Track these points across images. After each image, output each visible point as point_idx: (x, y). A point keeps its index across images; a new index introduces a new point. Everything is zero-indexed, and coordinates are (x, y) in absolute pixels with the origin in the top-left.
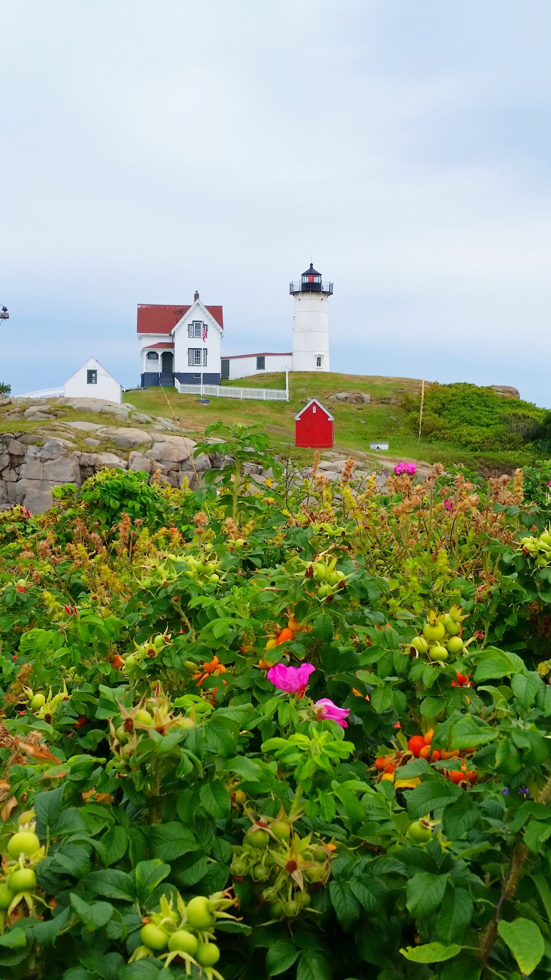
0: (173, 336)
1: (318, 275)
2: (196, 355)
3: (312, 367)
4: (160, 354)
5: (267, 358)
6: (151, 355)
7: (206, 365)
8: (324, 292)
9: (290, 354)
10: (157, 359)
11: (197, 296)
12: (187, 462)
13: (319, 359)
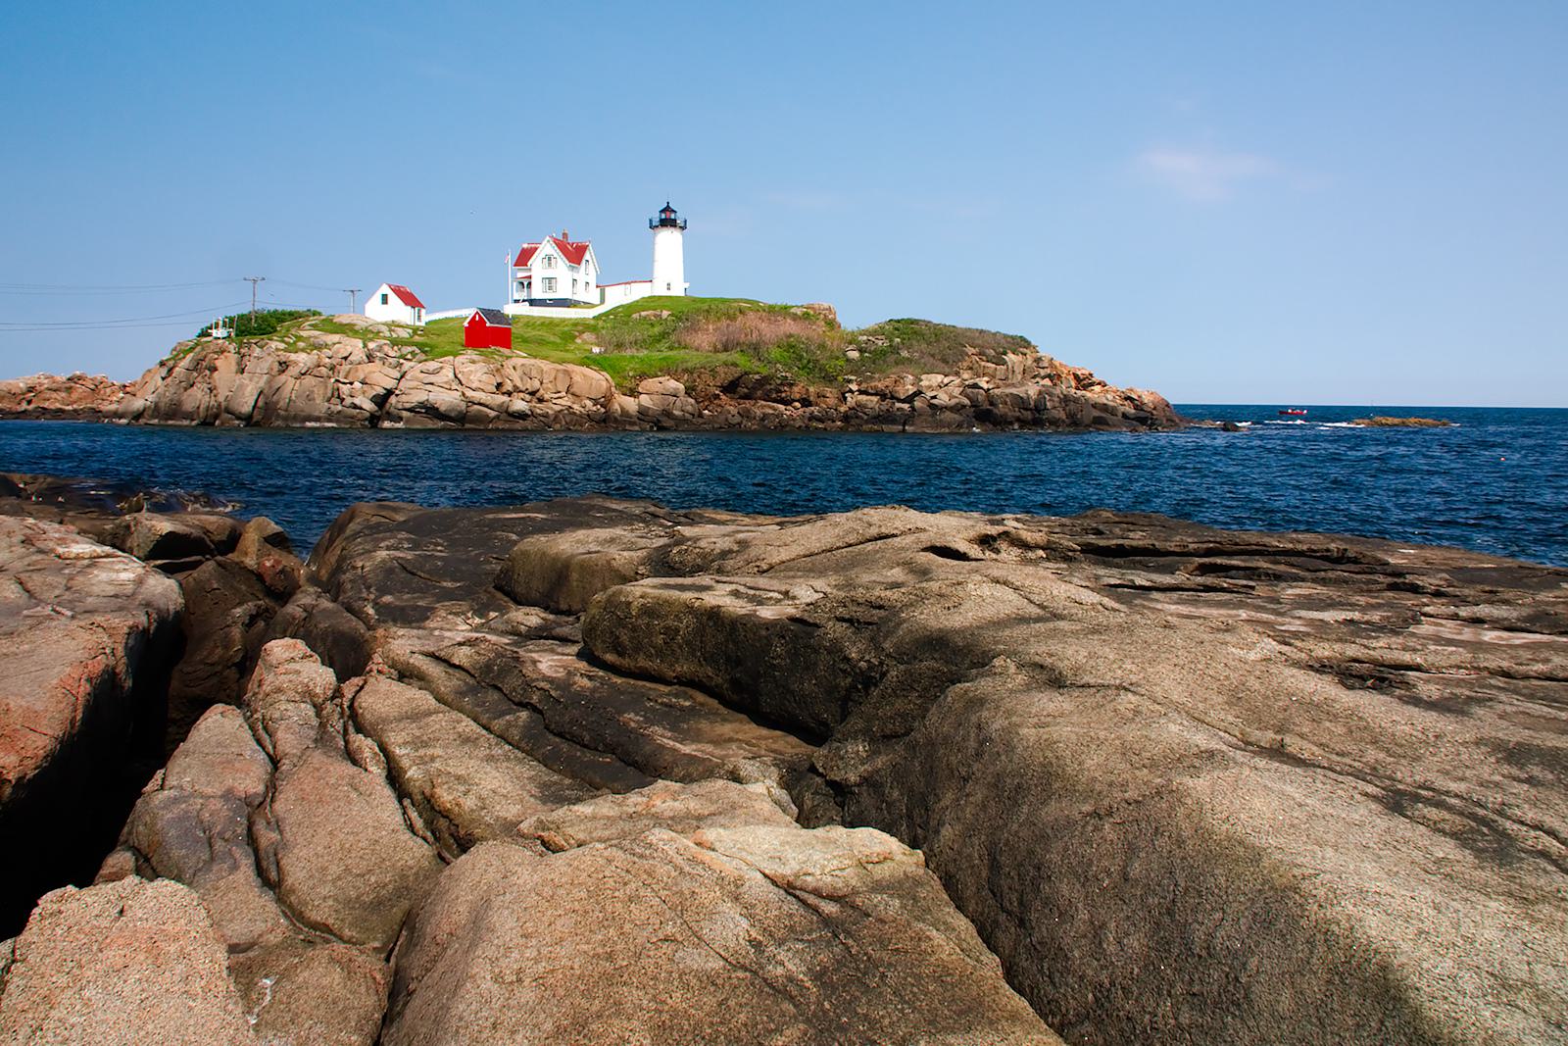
2: (550, 281)
3: (665, 293)
4: (526, 284)
11: (565, 235)
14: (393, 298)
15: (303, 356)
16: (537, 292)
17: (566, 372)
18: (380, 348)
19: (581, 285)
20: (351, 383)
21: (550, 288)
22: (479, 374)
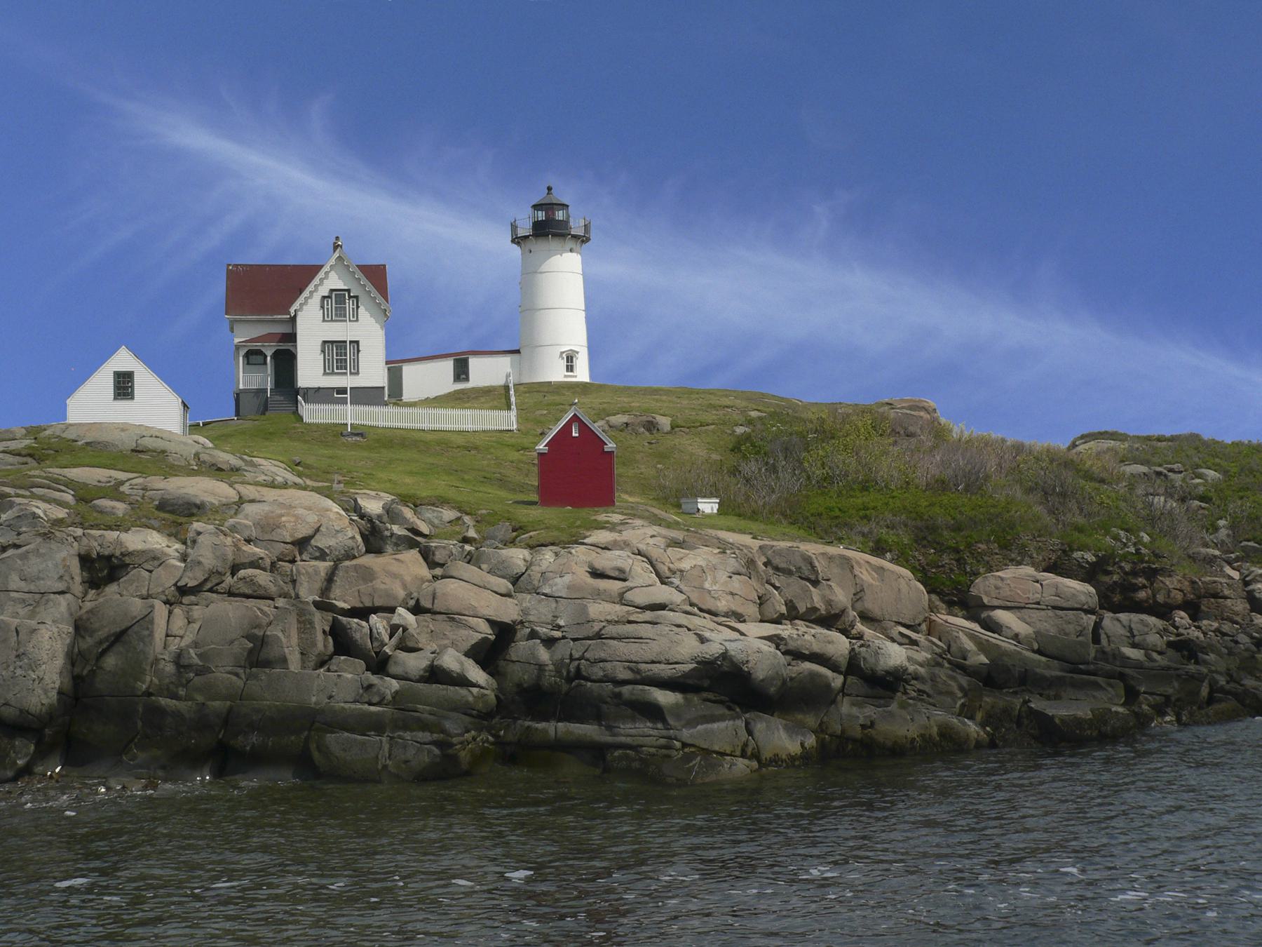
0: (293, 320)
1: (564, 206)
4: (269, 354)
5: (474, 363)
6: (253, 356)
7: (358, 373)
8: (574, 237)
9: (518, 352)
10: (265, 363)
12: (313, 542)
15: (154, 540)
17: (847, 563)
20: (375, 610)
21: (342, 364)
22: (722, 576)
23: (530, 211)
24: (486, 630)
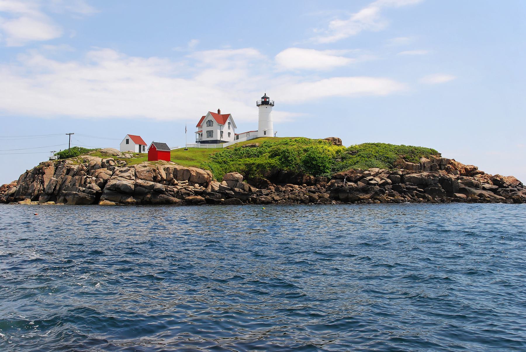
1: (268, 98)
3: (262, 135)
11: (219, 111)
13: (265, 132)
14: (131, 141)
16: (205, 138)
18: (108, 162)
19: (225, 135)
22: (145, 172)
23: (261, 99)
24: (102, 180)
